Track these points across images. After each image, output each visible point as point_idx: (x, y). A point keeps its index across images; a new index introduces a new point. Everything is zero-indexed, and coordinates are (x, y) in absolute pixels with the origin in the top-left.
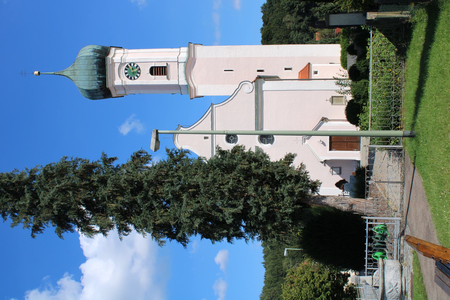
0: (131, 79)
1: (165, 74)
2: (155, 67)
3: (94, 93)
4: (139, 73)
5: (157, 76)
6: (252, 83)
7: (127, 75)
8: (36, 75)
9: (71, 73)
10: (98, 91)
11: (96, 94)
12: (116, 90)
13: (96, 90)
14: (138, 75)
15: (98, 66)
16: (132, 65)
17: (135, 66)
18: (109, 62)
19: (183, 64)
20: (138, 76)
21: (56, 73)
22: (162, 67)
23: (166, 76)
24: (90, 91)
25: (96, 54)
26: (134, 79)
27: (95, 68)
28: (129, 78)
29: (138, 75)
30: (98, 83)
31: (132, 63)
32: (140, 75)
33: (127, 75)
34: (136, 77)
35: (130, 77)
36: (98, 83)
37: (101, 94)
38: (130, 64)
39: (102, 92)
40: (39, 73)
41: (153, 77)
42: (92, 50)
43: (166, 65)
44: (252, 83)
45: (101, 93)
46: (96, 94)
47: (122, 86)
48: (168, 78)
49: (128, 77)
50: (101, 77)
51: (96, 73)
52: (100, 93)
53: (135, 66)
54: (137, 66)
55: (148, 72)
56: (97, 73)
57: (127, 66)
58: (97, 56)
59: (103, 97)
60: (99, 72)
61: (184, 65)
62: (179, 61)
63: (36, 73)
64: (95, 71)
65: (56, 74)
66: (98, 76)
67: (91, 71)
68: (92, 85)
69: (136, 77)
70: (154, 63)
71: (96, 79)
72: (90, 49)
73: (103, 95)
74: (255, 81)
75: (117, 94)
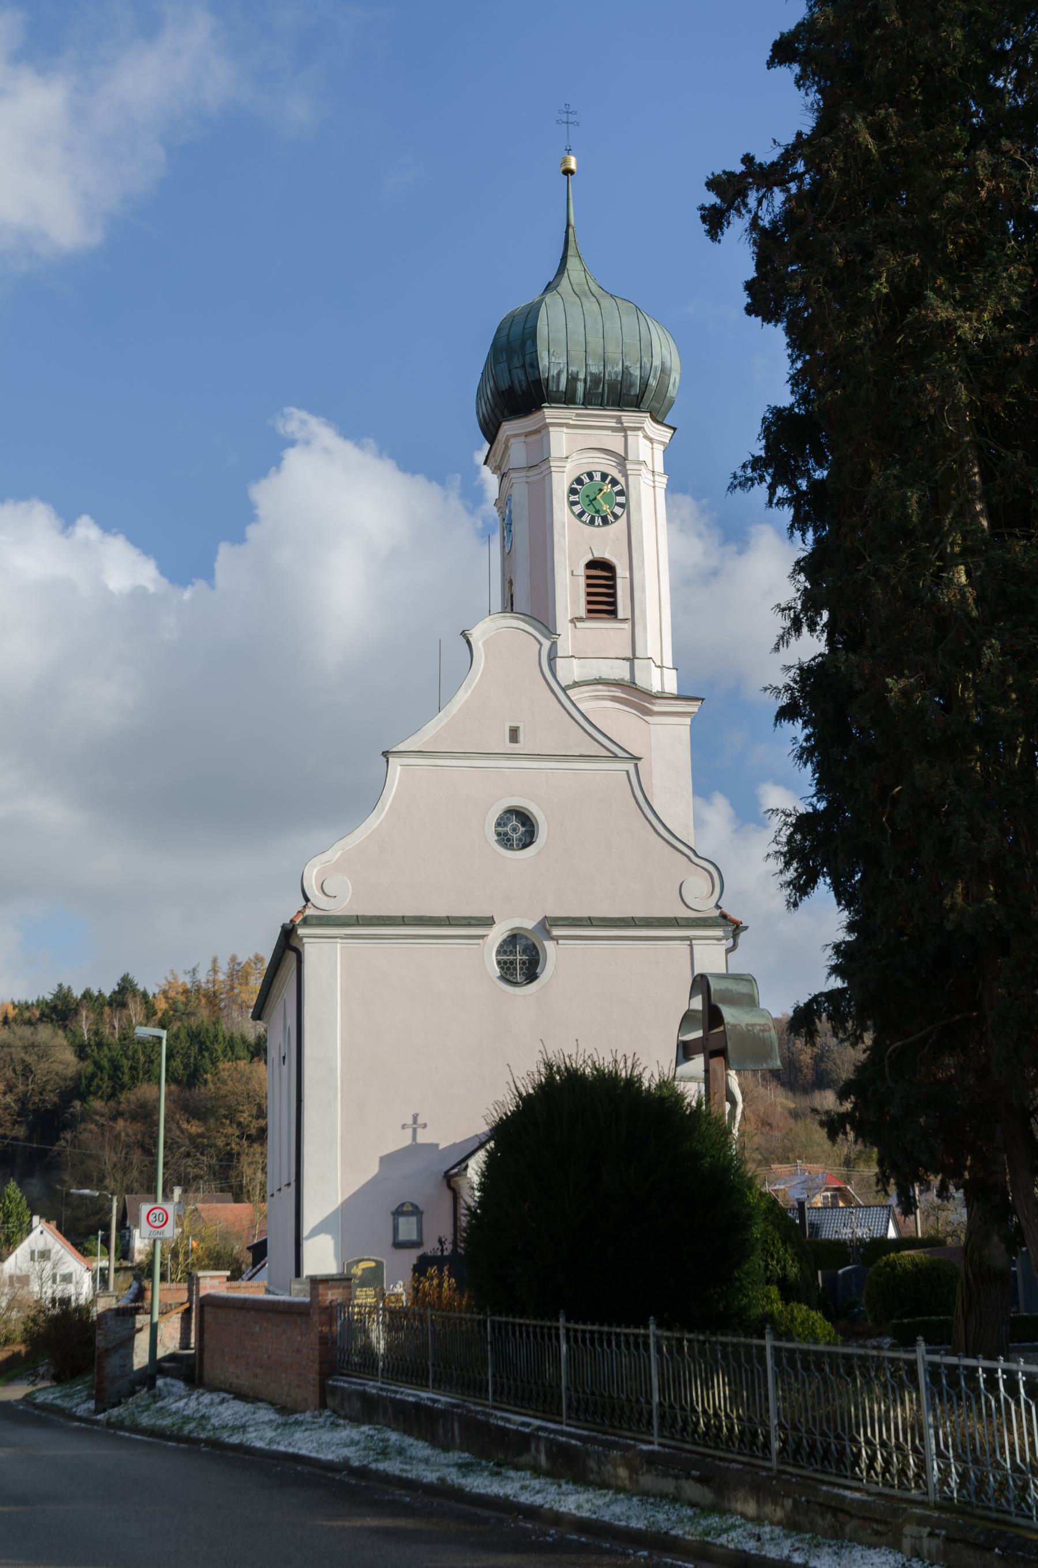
0: (573, 491)
1: (589, 611)
2: (613, 578)
3: (524, 356)
4: (592, 522)
5: (582, 581)
6: (718, 907)
7: (586, 480)
8: (565, 161)
9: (578, 284)
10: (529, 370)
11: (517, 362)
12: (528, 434)
13: (534, 365)
14: (586, 518)
15: (616, 380)
16: (621, 499)
17: (618, 510)
18: (629, 418)
19: (627, 677)
20: (584, 518)
21: (571, 230)
22: (614, 604)
23: (583, 613)
24: (529, 343)
25: (654, 378)
26: (573, 503)
27: (609, 368)
28: (575, 486)
29: (586, 518)
30: (559, 374)
31: (627, 499)
32: (584, 523)
33: (586, 480)
34: (577, 509)
35: (578, 487)
36: (559, 374)
37: (516, 382)
38: (621, 493)
39: (524, 385)
40: (568, 172)
41: (581, 571)
42: (668, 364)
43: (620, 616)
44: (718, 907)
45: (520, 382)
46: (517, 362)
47: (547, 460)
48: (575, 620)
49: (579, 481)
50: (580, 386)
51: (593, 369)
52: (523, 378)
53: (618, 510)
54: (616, 517)
55: (598, 554)
56: (592, 374)
57: (614, 482)
58: (651, 380)
59: (504, 385)
60: (597, 380)
61: (623, 680)
62: (636, 660)
63: (573, 165)
64: (602, 368)
65: (567, 232)
66: (582, 376)
67: (601, 351)
68: (551, 351)
69: (577, 509)
70: (628, 575)
71: (573, 369)
72: (669, 358)
73: (511, 388)
74: (724, 916)
75: (512, 441)
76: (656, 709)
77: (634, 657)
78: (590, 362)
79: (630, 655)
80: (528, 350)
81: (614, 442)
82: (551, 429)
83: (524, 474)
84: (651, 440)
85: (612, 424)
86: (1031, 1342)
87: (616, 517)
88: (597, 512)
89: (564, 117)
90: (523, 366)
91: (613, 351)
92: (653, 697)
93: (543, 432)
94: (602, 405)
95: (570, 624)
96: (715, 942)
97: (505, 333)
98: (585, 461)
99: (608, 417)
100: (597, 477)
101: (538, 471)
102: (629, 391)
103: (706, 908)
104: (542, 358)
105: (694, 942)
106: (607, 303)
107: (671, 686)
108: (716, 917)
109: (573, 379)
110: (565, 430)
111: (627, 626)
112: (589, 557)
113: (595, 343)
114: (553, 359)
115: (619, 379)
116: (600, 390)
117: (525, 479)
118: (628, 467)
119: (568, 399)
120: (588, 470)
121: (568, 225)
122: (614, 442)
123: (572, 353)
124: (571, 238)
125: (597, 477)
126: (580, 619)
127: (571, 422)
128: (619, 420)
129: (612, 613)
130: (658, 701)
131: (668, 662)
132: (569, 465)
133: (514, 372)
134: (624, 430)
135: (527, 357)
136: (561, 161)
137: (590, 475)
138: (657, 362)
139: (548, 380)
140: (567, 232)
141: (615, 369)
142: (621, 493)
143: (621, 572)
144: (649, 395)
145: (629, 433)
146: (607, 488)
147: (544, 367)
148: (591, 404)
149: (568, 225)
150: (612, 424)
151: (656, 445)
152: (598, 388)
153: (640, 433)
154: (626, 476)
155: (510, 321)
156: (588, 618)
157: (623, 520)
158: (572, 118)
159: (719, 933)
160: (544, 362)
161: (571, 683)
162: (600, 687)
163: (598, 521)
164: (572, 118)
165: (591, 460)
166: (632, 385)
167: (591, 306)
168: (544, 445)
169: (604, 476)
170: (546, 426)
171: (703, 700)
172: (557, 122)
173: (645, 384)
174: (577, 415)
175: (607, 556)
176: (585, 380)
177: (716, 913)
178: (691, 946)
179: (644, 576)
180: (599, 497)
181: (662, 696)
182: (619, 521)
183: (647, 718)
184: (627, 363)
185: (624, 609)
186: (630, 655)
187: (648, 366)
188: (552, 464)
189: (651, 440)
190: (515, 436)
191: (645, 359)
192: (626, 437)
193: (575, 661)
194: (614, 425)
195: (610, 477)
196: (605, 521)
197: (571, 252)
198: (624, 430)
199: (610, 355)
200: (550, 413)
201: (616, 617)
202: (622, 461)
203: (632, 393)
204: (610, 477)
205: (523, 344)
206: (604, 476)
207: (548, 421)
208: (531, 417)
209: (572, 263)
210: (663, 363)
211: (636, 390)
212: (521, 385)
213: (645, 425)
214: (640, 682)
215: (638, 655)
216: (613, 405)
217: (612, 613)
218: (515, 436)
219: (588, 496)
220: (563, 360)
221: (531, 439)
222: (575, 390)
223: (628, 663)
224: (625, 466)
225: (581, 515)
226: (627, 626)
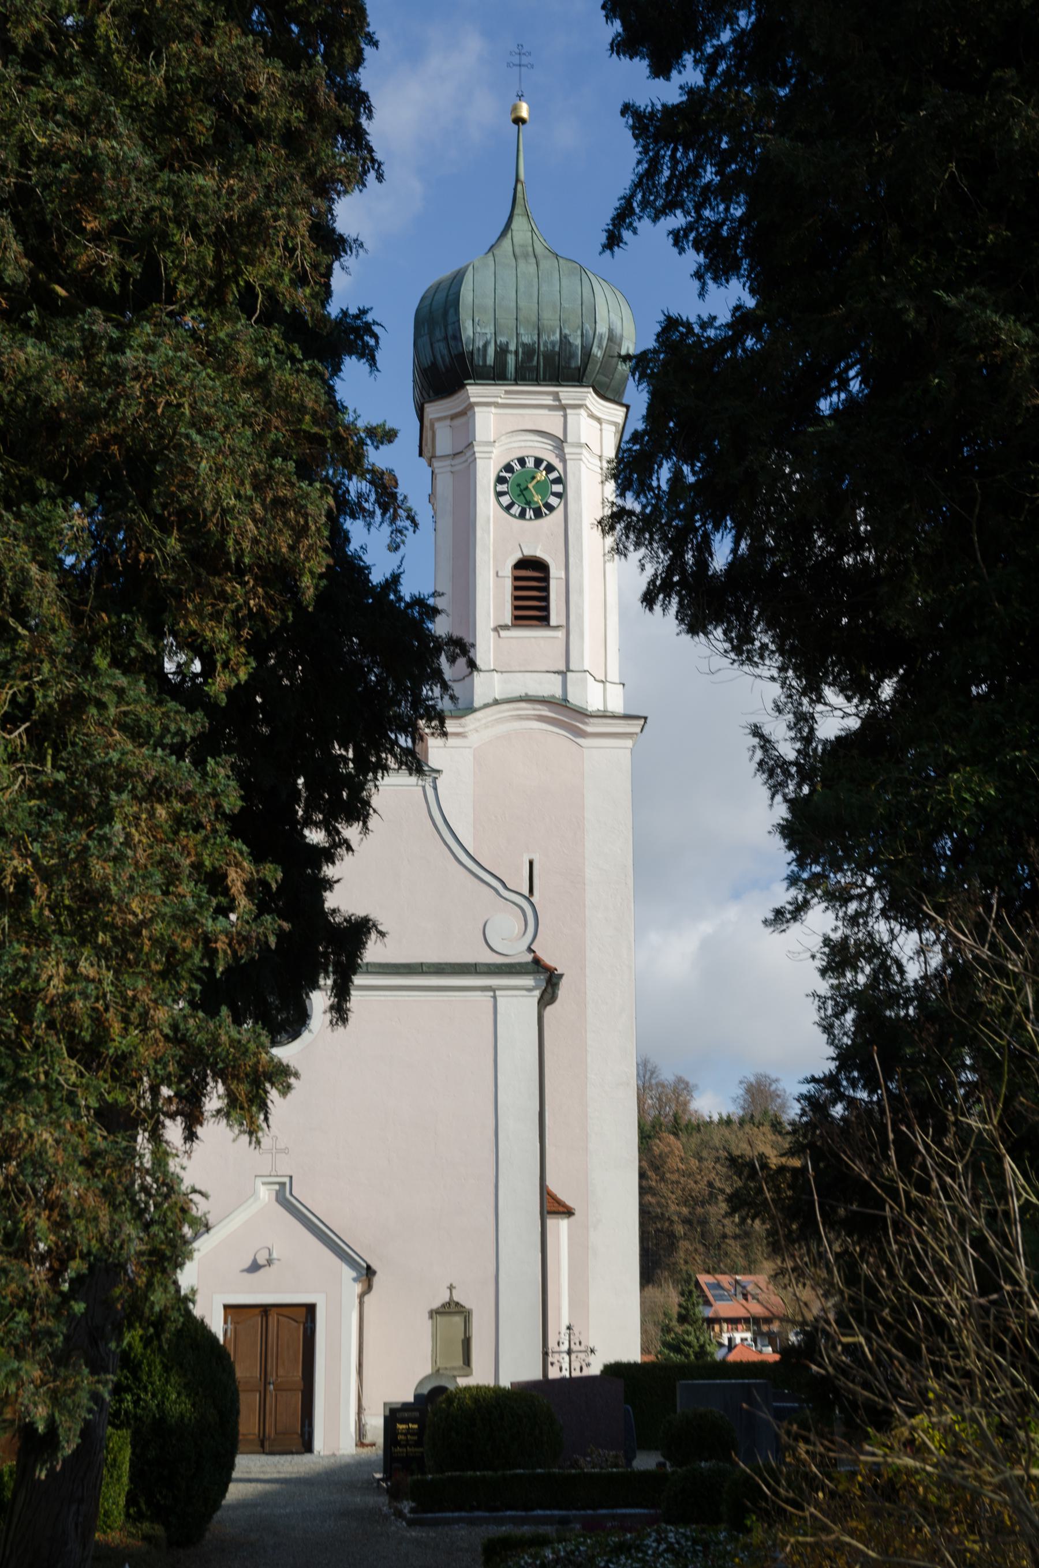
0: (501, 480)
1: (516, 618)
2: (546, 579)
3: (446, 327)
4: (522, 515)
5: (508, 584)
6: (530, 950)
7: (517, 467)
8: (515, 108)
9: (522, 246)
10: (452, 343)
11: (439, 334)
12: (453, 417)
13: (457, 337)
14: (516, 510)
15: (553, 351)
16: (558, 488)
17: (553, 501)
18: (568, 394)
19: (558, 693)
20: (513, 511)
21: (519, 187)
22: (546, 609)
23: (508, 620)
24: (452, 311)
25: (600, 347)
26: (499, 494)
27: (544, 337)
28: (504, 474)
29: (516, 510)
30: (486, 346)
31: (565, 488)
32: (514, 516)
33: (517, 467)
34: (506, 500)
35: (507, 475)
36: (486, 346)
37: (439, 357)
38: (558, 481)
39: (447, 360)
40: (519, 121)
41: (507, 571)
42: (618, 331)
43: (553, 622)
44: (530, 950)
45: (442, 357)
46: (439, 334)
47: (470, 445)
48: (499, 628)
49: (508, 468)
50: (511, 360)
51: (526, 339)
52: (445, 352)
53: (553, 501)
54: (551, 508)
55: (528, 552)
56: (524, 345)
57: (550, 468)
58: (595, 350)
59: (427, 362)
60: (529, 351)
61: (553, 697)
62: (569, 674)
63: (524, 112)
64: (535, 338)
65: (515, 189)
66: (512, 347)
67: (534, 318)
68: (476, 319)
69: (506, 500)
70: (563, 575)
71: (502, 339)
72: (619, 324)
73: (434, 364)
74: (537, 961)
75: (437, 425)
76: (589, 729)
77: (568, 670)
78: (522, 331)
79: (563, 668)
80: (451, 319)
81: (551, 422)
82: (477, 409)
83: (448, 462)
84: (599, 420)
85: (549, 401)
86: (593, 1509)
87: (551, 508)
88: (528, 503)
89: (516, 59)
90: (446, 338)
91: (550, 318)
92: (583, 714)
93: (469, 413)
94: (537, 381)
95: (492, 633)
96: (524, 993)
97: (428, 302)
98: (516, 445)
99: (542, 394)
100: (530, 463)
101: (464, 459)
102: (569, 363)
103: (517, 953)
104: (465, 329)
105: (498, 993)
106: (548, 264)
107: (616, 705)
108: (527, 964)
109: (502, 351)
110: (493, 410)
111: (560, 634)
112: (518, 556)
113: (528, 307)
114: (478, 329)
115: (557, 349)
116: (535, 363)
117: (449, 469)
118: (567, 450)
119: (496, 375)
120: (520, 455)
121: (517, 180)
122: (551, 422)
123: (501, 321)
124: (519, 195)
125: (530, 463)
126: (505, 627)
127: (500, 401)
128: (556, 397)
129: (542, 618)
130: (592, 720)
131: (614, 675)
132: (496, 451)
133: (436, 345)
134: (563, 408)
135: (450, 328)
136: (510, 108)
137: (522, 461)
138: (602, 329)
139: (472, 353)
140: (515, 189)
141: (552, 338)
142: (558, 481)
143: (556, 573)
144: (593, 369)
145: (569, 411)
146: (541, 475)
147: (468, 338)
148: (524, 379)
149: (517, 180)
150: (549, 401)
151: (605, 426)
152: (532, 360)
153: (582, 412)
154: (564, 461)
155: (437, 288)
156: (514, 626)
157: (559, 513)
158: (525, 60)
159: (528, 981)
160: (468, 330)
161: (490, 701)
162: (523, 705)
163: (530, 513)
164: (525, 60)
165: (523, 444)
166: (572, 356)
167: (528, 268)
168: (469, 430)
169: (538, 462)
170: (471, 407)
171: (646, 718)
172: (508, 65)
173: (587, 354)
174: (507, 392)
175: (540, 553)
176: (516, 353)
177: (529, 958)
178: (495, 997)
179: (582, 576)
180: (530, 486)
181: (604, 715)
182: (555, 513)
183: (580, 741)
184: (566, 331)
185: (558, 614)
186: (563, 668)
187: (591, 333)
188: (476, 449)
189: (599, 420)
190: (440, 419)
191: (587, 326)
192: (565, 416)
193: (495, 674)
194: (551, 403)
195: (545, 464)
196: (538, 514)
197: (518, 210)
198: (563, 408)
199: (545, 322)
200: (475, 392)
201: (548, 625)
202: (560, 444)
203: (573, 365)
204: (545, 464)
205: (445, 313)
206: (538, 462)
207: (472, 400)
208: (456, 396)
209: (519, 224)
210: (611, 331)
211: (577, 362)
212: (444, 361)
213: (587, 403)
214: (573, 699)
215: (572, 667)
216: (550, 380)
217: (542, 618)
218: (440, 419)
219: (519, 485)
220: (489, 330)
221: (457, 422)
222: (504, 364)
223: (559, 678)
224: (562, 449)
225: (508, 508)
226: (560, 634)
